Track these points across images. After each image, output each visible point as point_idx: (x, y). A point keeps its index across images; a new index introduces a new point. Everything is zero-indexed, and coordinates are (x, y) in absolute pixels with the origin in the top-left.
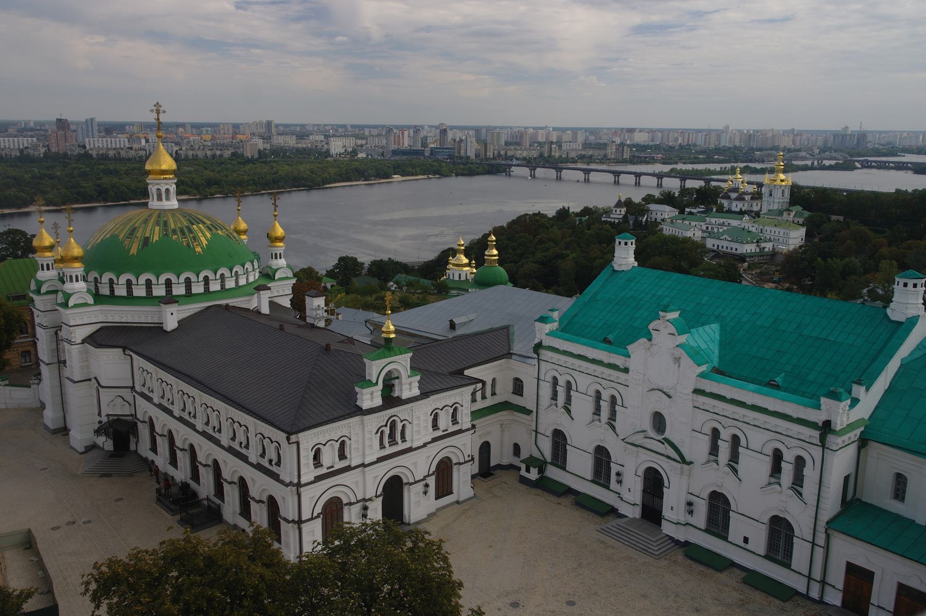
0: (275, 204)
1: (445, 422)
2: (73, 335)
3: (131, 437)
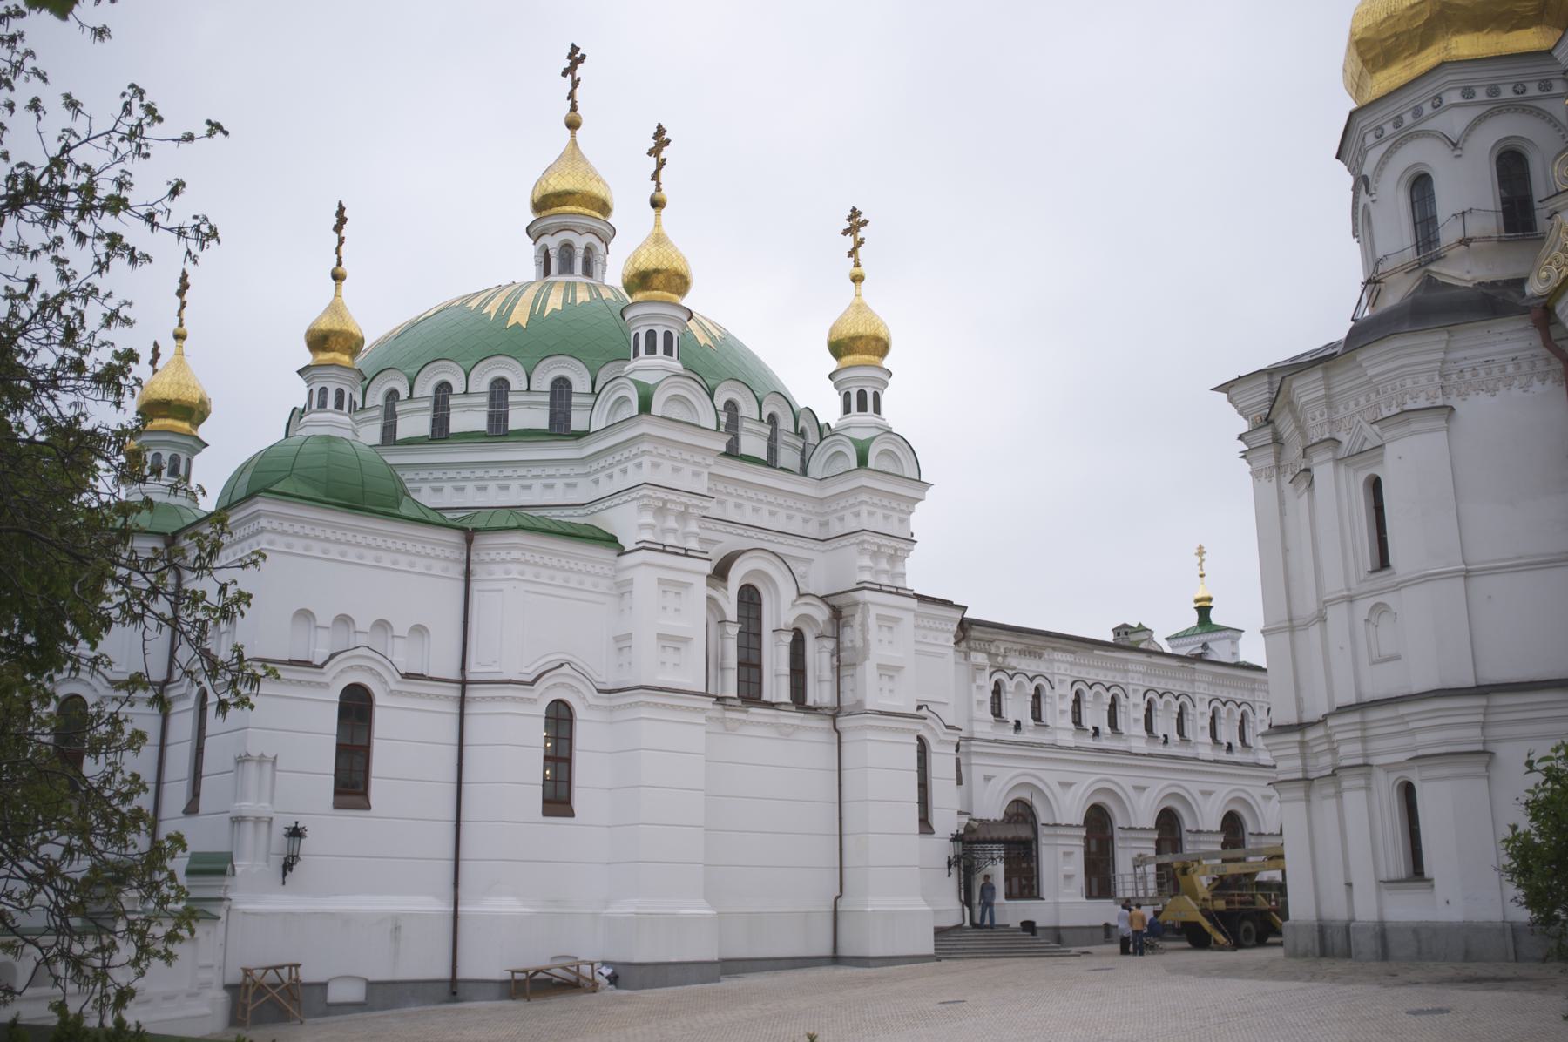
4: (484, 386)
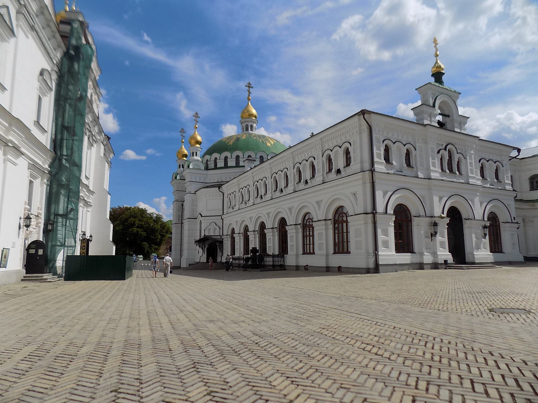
1: (490, 174)
3: (218, 250)
4: (223, 158)
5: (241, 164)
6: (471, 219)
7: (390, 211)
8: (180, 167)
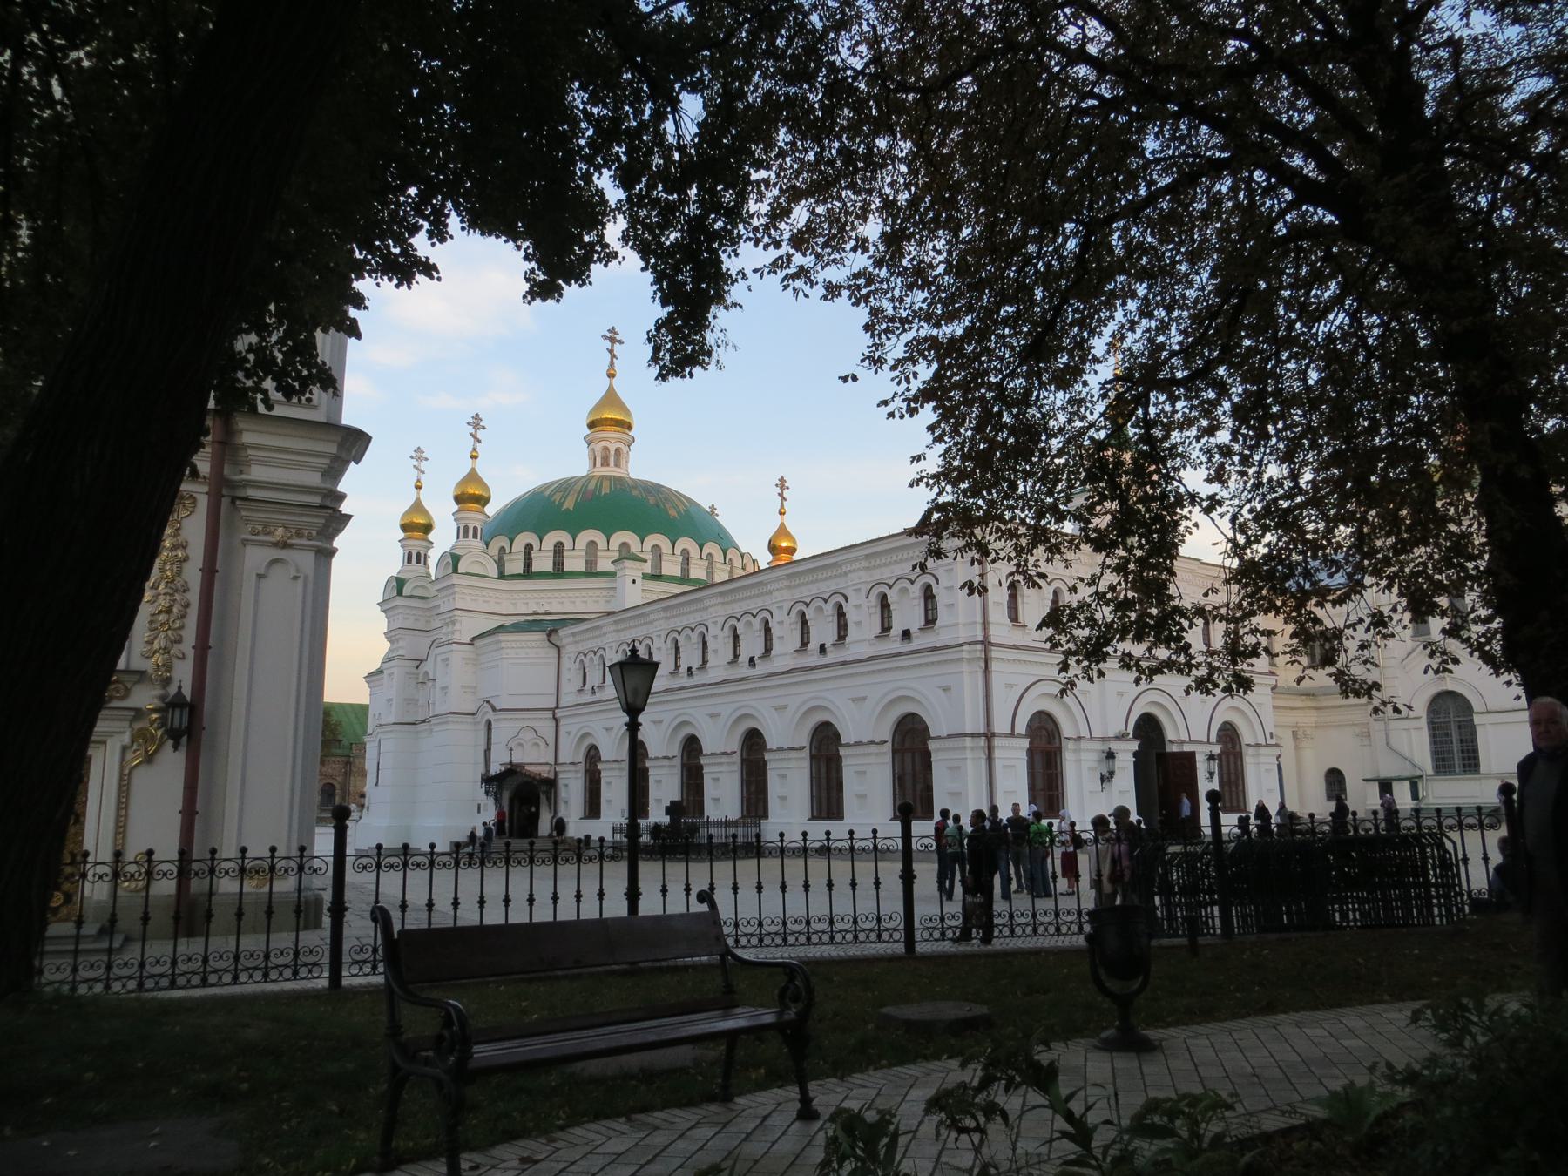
0: (781, 495)
2: (457, 626)
5: (604, 564)
6: (1183, 742)
7: (1021, 728)
8: (409, 561)
